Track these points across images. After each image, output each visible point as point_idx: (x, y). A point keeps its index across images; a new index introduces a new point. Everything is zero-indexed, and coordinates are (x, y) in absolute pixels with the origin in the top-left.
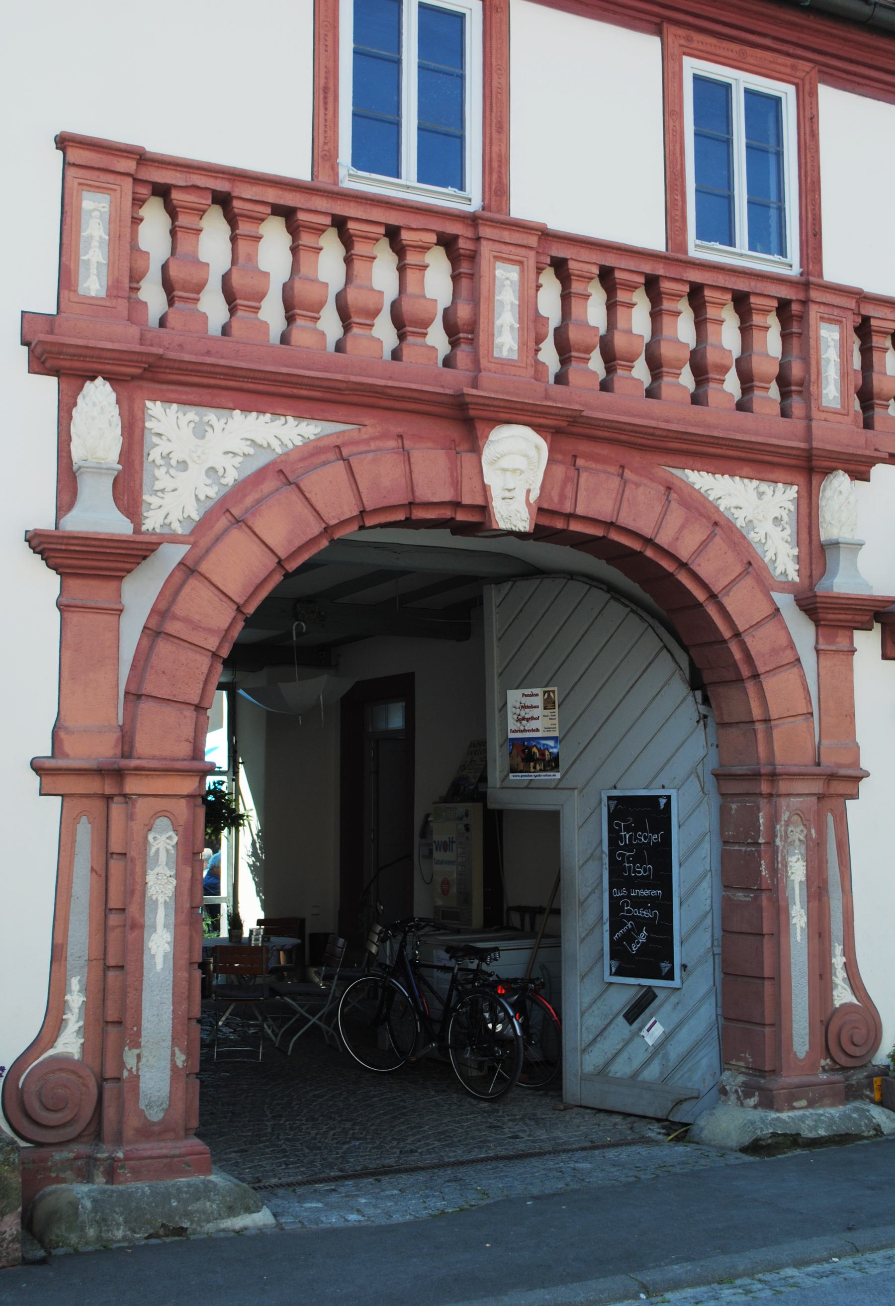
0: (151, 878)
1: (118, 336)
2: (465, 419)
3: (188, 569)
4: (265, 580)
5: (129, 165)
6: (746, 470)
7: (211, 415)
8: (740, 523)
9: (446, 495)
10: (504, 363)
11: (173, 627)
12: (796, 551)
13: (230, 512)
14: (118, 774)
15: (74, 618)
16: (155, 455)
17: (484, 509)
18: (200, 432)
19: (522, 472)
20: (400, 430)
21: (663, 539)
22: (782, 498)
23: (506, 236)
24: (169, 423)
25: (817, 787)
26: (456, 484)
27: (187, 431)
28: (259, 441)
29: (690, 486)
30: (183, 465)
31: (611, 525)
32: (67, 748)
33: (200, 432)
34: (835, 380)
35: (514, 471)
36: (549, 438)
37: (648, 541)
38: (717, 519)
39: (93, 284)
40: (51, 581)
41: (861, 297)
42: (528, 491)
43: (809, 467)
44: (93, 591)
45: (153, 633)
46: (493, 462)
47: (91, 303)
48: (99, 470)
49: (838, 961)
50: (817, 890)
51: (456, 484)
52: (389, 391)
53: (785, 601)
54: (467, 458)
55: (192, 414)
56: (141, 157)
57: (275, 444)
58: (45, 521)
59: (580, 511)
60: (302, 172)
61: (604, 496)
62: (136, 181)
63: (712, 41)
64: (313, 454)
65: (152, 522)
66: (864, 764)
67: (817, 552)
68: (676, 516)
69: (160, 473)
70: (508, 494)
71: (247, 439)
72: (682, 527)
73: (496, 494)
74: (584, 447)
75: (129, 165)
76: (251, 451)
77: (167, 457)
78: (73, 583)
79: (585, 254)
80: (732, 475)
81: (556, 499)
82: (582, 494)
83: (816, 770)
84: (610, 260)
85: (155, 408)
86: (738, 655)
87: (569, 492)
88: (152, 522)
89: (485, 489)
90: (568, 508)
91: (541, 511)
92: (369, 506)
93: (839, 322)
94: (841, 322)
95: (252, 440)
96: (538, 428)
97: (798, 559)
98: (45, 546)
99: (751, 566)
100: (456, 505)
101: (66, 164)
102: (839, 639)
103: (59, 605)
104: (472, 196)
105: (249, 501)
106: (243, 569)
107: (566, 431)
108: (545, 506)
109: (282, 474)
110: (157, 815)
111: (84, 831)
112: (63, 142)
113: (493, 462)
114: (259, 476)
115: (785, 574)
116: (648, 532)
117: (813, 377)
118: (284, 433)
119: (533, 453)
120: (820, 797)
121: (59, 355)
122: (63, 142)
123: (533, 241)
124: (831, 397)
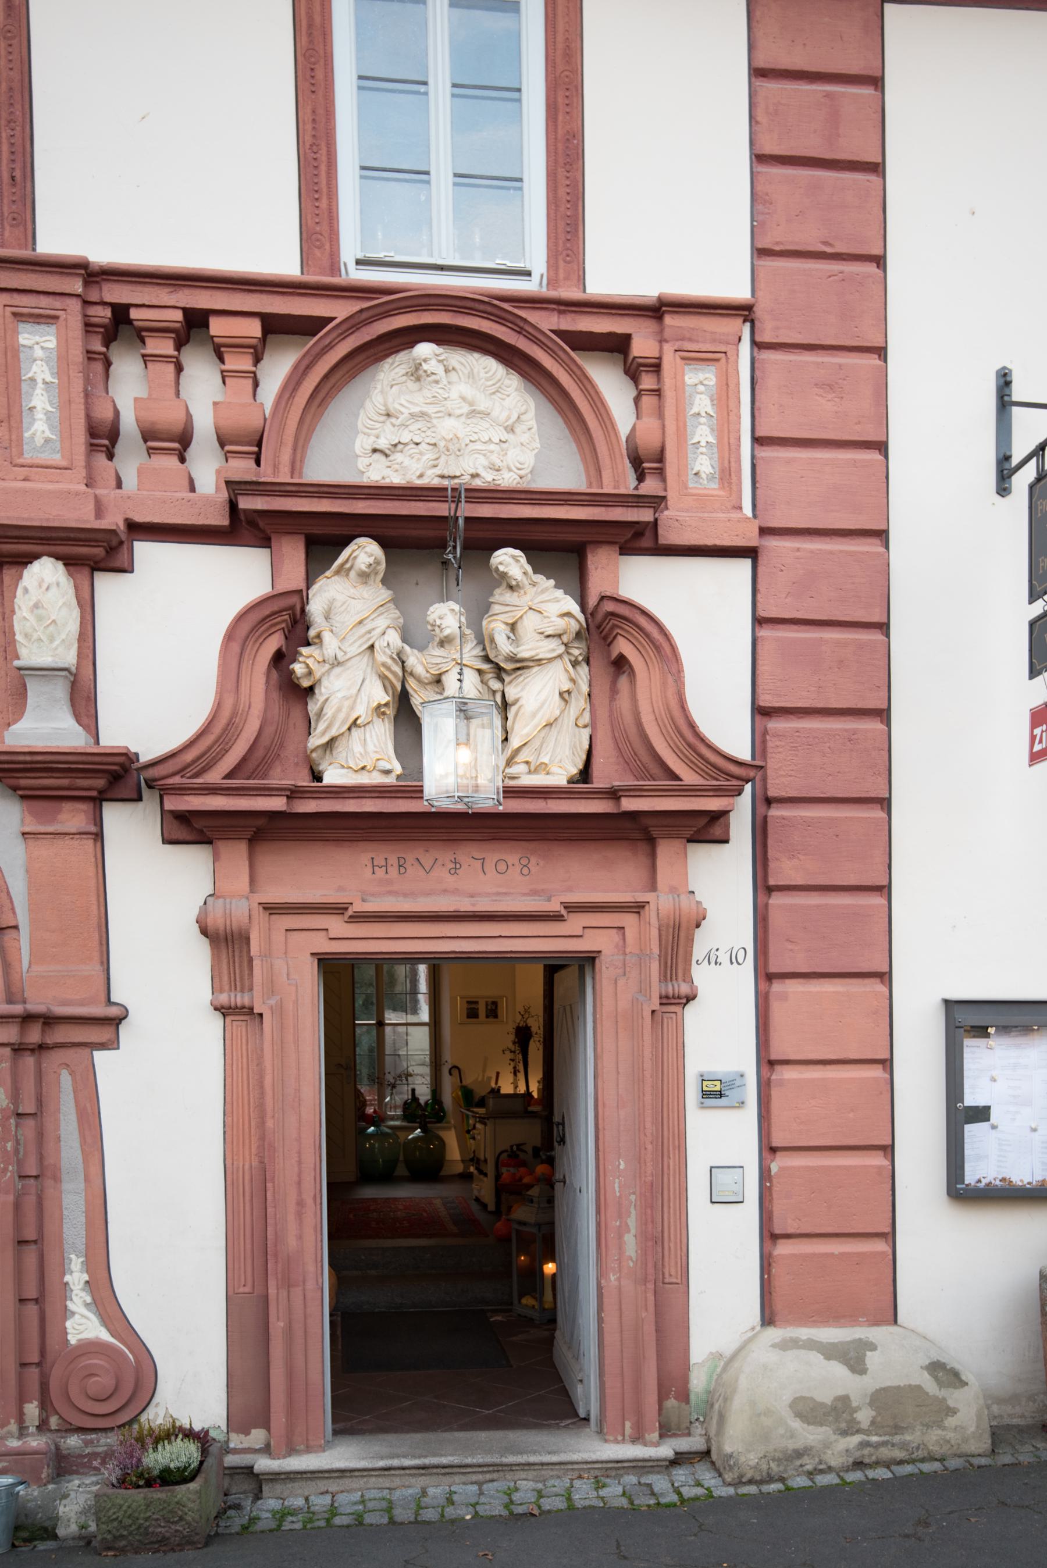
34: (47, 413)
41: (94, 275)
93: (51, 319)
94: (56, 318)
102: (63, 816)
124: (39, 441)
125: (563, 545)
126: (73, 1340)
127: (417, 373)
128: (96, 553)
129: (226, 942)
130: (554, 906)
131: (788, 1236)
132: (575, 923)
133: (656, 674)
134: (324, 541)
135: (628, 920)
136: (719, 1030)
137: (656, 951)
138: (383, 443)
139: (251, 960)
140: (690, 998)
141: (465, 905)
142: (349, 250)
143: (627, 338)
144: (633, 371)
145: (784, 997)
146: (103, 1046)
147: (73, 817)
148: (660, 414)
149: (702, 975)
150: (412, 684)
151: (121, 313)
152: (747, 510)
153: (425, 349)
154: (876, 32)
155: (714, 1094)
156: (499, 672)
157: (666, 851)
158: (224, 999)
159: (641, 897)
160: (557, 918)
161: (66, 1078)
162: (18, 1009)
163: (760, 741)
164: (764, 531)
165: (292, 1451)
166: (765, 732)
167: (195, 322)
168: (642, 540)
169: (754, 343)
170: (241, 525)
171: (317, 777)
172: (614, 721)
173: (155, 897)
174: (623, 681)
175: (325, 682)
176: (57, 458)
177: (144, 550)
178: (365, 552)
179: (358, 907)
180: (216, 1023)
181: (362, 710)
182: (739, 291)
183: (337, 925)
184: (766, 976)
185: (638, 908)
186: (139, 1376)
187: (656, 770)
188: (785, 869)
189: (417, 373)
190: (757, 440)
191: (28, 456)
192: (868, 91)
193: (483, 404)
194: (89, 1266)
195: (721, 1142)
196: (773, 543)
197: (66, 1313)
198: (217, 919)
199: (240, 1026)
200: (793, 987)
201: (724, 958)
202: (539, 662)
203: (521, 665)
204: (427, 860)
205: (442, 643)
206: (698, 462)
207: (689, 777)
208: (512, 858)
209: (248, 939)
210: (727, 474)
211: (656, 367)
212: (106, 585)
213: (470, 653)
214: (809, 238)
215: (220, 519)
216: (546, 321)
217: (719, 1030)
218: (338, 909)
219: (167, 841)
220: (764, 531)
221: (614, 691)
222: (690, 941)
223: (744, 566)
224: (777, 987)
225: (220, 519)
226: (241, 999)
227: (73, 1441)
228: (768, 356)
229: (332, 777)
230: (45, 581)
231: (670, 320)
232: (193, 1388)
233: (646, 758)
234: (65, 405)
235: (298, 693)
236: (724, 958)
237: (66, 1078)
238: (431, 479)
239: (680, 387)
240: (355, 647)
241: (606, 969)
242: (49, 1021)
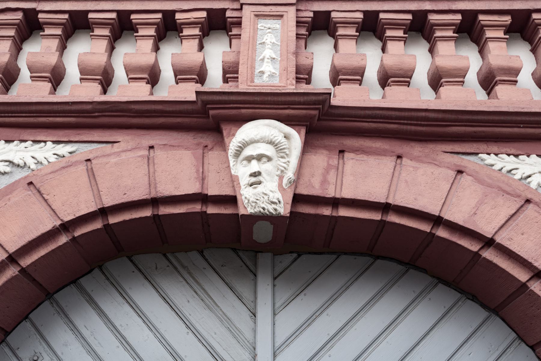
19: (269, 159)
28: (16, 161)
35: (259, 158)
36: (303, 131)
37: (438, 221)
38: (529, 196)
42: (281, 178)
46: (238, 153)
52: (133, 107)
59: (347, 193)
64: (65, 165)
70: (253, 179)
71: (6, 161)
72: (481, 203)
76: (8, 169)
81: (317, 185)
82: (348, 180)
89: (234, 180)
90: (331, 193)
95: (10, 162)
100: (202, 198)
107: (321, 122)
108: (303, 191)
113: (238, 153)
116: (434, 210)
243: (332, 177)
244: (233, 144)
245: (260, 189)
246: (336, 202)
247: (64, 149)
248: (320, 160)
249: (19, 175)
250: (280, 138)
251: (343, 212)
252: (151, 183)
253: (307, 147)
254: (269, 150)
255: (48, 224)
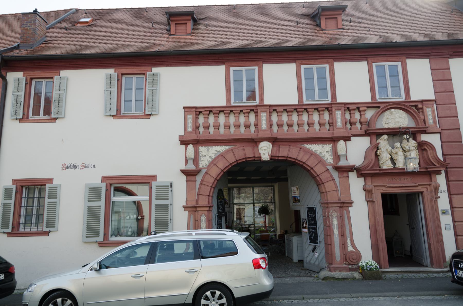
0: (201, 224)
1: (194, 137)
2: (255, 142)
3: (206, 173)
4: (220, 173)
5: (194, 109)
6: (319, 143)
7: (210, 148)
8: (318, 153)
9: (253, 156)
10: (264, 131)
11: (204, 183)
12: (332, 157)
13: (213, 163)
14: (195, 207)
15: (189, 182)
16: (201, 155)
17: (260, 157)
18: (208, 150)
20: (242, 145)
21: (299, 159)
22: (328, 147)
23: (263, 108)
24: (202, 149)
25: (339, 205)
26: (254, 154)
27: (206, 151)
29: (306, 148)
30: (205, 156)
31: (287, 157)
32: (188, 203)
33: (208, 150)
39: (190, 129)
40: (185, 177)
41: (345, 104)
43: (334, 140)
44: (192, 178)
45: (201, 184)
46: (260, 149)
47: (190, 133)
48: (190, 159)
49: (349, 241)
50: (342, 226)
51: (254, 154)
53: (330, 168)
54: (256, 148)
55: (206, 148)
56: (196, 108)
57: (221, 151)
58: (183, 168)
59: (280, 155)
60: (224, 104)
61: (285, 152)
62: (196, 112)
63: (307, 61)
64: (227, 151)
65: (201, 166)
66: (352, 200)
67: (337, 157)
68: (302, 154)
69: (202, 158)
73: (262, 154)
74: (281, 143)
75: (194, 109)
77: (202, 155)
78: (188, 177)
79: (280, 108)
80: (315, 144)
82: (280, 152)
83: (339, 201)
84: (285, 108)
85: (200, 148)
86: (319, 179)
87: (278, 152)
88: (201, 166)
89: (260, 154)
90: (277, 155)
91: (271, 156)
92: (238, 159)
96: (269, 141)
97: (333, 159)
98: (184, 172)
99: (321, 161)
100: (254, 157)
101: (185, 111)
103: (187, 181)
104: (257, 102)
105: (216, 161)
106: (215, 172)
108: (272, 155)
109: (222, 155)
110: (202, 214)
111: (192, 217)
112: (184, 108)
113: (260, 149)
114: (218, 157)
115: (330, 162)
116: (295, 157)
117: (334, 122)
118: (222, 148)
119: (268, 146)
120: (340, 207)
121: (184, 142)
122: (184, 108)
123: (268, 107)
125: (414, 134)
126: (349, 250)
127: (391, 113)
128: (347, 139)
129: (368, 191)
130: (417, 185)
131: (460, 235)
132: (420, 187)
133: (431, 151)
134: (379, 134)
135: (428, 187)
136: (443, 202)
137: (433, 190)
138: (387, 122)
139: (372, 194)
140: (439, 197)
141: (404, 185)
142: (378, 97)
143: (417, 105)
144: (418, 109)
145: (454, 198)
146: (350, 207)
147: (345, 175)
148: (423, 115)
149: (439, 194)
150: (392, 154)
151: (348, 108)
152: (438, 127)
153: (393, 110)
154: (448, 63)
155: (444, 213)
156: (405, 151)
157: (433, 176)
158: (368, 199)
159: (431, 183)
160: (417, 186)
161: (345, 211)
162: (341, 201)
163: (445, 159)
164: (442, 130)
165: (385, 268)
166: (445, 158)
167: (358, 108)
168: (425, 132)
169: (436, 104)
170: (367, 134)
171: (380, 167)
172: (423, 158)
173: (356, 185)
174: (425, 152)
175: (382, 155)
176: (341, 127)
177: (353, 138)
178: (385, 137)
179: (388, 186)
180: (366, 203)
181: (388, 158)
182: (433, 98)
183: (384, 188)
184: (450, 194)
185: (429, 185)
186: (359, 257)
187: (431, 164)
188: (451, 178)
189: (391, 113)
190: (438, 117)
191: (338, 127)
192: (448, 70)
193: (401, 116)
194: (350, 240)
195: (446, 221)
196: (443, 131)
197: (347, 247)
198: (367, 188)
199: (370, 203)
200: (455, 196)
201: (443, 192)
202: (412, 150)
203: (410, 151)
204: (396, 179)
205: (397, 148)
206: (430, 121)
207: (437, 165)
208: (409, 178)
209: (372, 191)
210: (435, 122)
211: (422, 109)
212: (348, 142)
213: (401, 149)
214: (442, 90)
215: (364, 133)
216: (407, 104)
217: (443, 202)
218: (385, 186)
219: (357, 177)
220: (442, 130)
221: (423, 154)
222: (438, 189)
223: (439, 134)
224: (452, 196)
225: (364, 133)
226: (371, 200)
227: (350, 266)
228: (438, 106)
229: (384, 168)
230: (342, 143)
231: (424, 103)
232: (367, 259)
233: (429, 162)
234: (342, 120)
235: (377, 156)
236: (443, 192)
237: (345, 211)
238: (394, 126)
239: (426, 111)
240: (385, 149)
241: (425, 194)
242: (343, 203)
243: (278, 152)
244: (260, 147)
245: (265, 156)
246: (278, 156)
247: (227, 147)
248: (275, 148)
249: (219, 153)
250: (268, 146)
251: (280, 158)
252: (245, 155)
253: (272, 146)
254: (265, 148)
255: (228, 164)
